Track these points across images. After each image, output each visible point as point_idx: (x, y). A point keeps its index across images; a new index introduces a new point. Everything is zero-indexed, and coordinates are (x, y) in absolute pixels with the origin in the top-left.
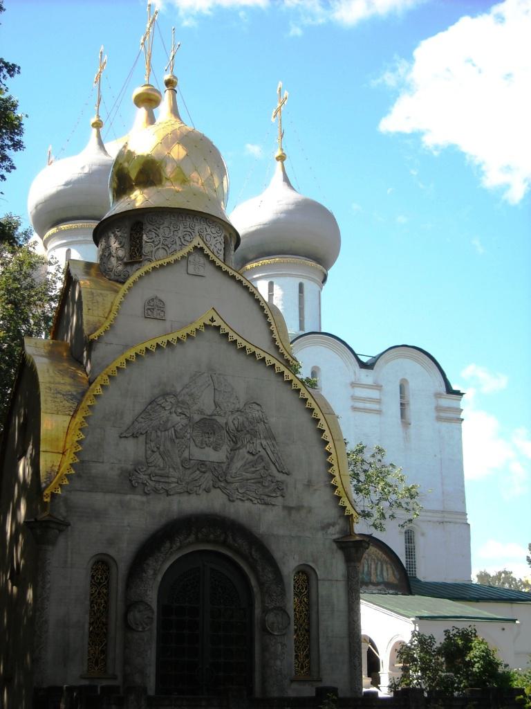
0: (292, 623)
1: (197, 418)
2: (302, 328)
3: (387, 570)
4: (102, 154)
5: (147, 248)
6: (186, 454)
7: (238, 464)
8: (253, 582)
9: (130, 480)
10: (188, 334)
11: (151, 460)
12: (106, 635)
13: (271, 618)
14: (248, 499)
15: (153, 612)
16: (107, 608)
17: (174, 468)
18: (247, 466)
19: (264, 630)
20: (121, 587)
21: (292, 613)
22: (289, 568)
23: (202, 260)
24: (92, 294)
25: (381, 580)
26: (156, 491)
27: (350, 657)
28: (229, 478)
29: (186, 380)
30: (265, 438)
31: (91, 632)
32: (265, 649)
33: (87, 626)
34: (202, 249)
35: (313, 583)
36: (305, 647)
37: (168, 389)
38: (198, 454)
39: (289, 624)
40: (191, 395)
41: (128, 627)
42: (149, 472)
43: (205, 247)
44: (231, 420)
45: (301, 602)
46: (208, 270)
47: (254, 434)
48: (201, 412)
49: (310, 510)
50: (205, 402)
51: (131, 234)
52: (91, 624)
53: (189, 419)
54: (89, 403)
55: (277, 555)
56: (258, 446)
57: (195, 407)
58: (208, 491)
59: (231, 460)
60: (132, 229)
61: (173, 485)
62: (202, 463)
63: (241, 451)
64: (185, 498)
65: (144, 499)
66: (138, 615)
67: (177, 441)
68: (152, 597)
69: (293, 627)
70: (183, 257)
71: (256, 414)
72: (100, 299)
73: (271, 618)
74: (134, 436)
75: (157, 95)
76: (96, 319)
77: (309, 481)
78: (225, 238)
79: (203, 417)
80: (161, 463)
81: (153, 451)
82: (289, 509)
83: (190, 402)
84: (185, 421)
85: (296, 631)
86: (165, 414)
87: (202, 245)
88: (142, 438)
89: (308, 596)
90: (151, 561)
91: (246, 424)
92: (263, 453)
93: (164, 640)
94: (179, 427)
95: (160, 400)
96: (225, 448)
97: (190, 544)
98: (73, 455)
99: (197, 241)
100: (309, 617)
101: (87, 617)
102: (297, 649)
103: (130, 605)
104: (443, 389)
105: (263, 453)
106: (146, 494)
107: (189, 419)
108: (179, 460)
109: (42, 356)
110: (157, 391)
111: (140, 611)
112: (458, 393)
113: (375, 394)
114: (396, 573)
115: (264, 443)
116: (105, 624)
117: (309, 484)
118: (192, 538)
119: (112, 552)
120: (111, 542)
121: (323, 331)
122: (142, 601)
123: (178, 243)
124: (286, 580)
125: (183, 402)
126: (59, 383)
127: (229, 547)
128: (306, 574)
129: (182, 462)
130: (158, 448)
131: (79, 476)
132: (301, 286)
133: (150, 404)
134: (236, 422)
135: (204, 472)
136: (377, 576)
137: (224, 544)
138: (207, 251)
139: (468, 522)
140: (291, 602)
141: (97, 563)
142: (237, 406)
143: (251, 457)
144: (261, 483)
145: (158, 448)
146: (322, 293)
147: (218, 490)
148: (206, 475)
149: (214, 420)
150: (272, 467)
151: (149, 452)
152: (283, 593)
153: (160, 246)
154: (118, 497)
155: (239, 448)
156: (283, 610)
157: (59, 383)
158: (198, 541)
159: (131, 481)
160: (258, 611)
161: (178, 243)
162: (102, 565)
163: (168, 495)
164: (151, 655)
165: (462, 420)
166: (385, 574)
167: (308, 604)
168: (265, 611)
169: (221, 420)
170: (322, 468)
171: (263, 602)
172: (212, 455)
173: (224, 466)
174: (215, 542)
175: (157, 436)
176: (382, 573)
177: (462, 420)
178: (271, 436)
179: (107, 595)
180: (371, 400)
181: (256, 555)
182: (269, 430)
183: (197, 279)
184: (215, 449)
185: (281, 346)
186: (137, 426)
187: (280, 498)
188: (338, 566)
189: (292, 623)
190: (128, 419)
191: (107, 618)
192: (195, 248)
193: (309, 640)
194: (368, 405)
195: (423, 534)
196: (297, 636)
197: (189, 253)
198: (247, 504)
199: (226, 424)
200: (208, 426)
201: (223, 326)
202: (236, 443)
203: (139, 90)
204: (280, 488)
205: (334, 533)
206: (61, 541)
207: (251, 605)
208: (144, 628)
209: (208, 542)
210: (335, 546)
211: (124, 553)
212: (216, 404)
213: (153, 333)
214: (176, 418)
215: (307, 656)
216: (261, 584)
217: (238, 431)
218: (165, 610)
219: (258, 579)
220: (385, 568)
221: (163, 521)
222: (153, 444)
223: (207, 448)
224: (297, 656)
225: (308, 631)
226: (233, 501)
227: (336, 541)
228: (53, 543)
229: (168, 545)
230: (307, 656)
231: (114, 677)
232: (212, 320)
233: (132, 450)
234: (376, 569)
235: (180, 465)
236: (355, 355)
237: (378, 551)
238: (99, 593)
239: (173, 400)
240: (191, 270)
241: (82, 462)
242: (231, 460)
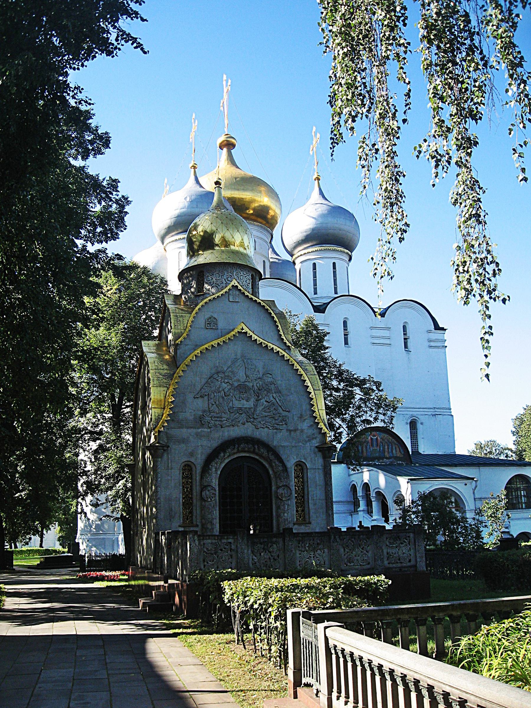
0: (294, 492)
1: (236, 384)
2: (336, 293)
3: (395, 448)
4: (198, 187)
6: (231, 405)
7: (260, 408)
9: (200, 421)
10: (229, 338)
11: (211, 409)
12: (192, 504)
13: (280, 491)
14: (266, 427)
15: (215, 490)
16: (191, 490)
17: (225, 413)
18: (265, 409)
19: (277, 497)
21: (293, 488)
22: (291, 464)
23: (237, 293)
24: (177, 316)
25: (392, 455)
27: (327, 510)
28: (255, 417)
29: (229, 363)
30: (275, 393)
31: (183, 503)
32: (278, 508)
33: (181, 499)
34: (237, 286)
35: (305, 471)
36: (302, 506)
37: (219, 369)
38: (237, 404)
39: (291, 494)
41: (202, 499)
42: (210, 416)
43: (238, 285)
44: (256, 384)
45: (299, 481)
46: (241, 299)
47: (269, 391)
48: (238, 380)
49: (302, 431)
50: (241, 375)
51: (198, 278)
52: (183, 498)
53: (232, 385)
54: (176, 381)
55: (284, 457)
56: (271, 397)
57: (235, 378)
58: (244, 424)
59: (256, 406)
60: (198, 275)
61: (224, 422)
62: (240, 409)
63: (262, 401)
65: (209, 430)
66: (208, 493)
67: (225, 398)
68: (215, 482)
69: (294, 495)
70: (226, 292)
71: (269, 380)
72: (181, 319)
73: (280, 491)
75: (233, 140)
76: (179, 331)
77: (301, 415)
78: (252, 275)
79: (239, 383)
80: (217, 410)
81: (213, 404)
82: (290, 431)
83: (232, 376)
84: (229, 387)
85: (296, 497)
87: (237, 284)
88: (206, 398)
89: (303, 478)
90: (213, 464)
91: (264, 385)
92: (274, 401)
93: (223, 504)
94: (226, 390)
95: (215, 376)
96: (253, 400)
97: (234, 453)
98: (169, 410)
99: (234, 282)
100: (303, 489)
101: (181, 495)
102: (297, 507)
103: (203, 488)
104: (433, 327)
105: (274, 401)
106: (210, 428)
108: (227, 409)
109: (153, 353)
110: (213, 371)
111: (208, 491)
112: (443, 329)
113: (386, 333)
114: (402, 450)
115: (274, 395)
116: (192, 498)
117: (301, 417)
118: (235, 451)
119: (193, 460)
120: (192, 454)
121: (350, 294)
122: (209, 486)
123: (224, 282)
124: (289, 470)
125: (228, 376)
126: (160, 369)
127: (257, 454)
128: (301, 466)
129: (229, 409)
130: (215, 402)
131: (172, 420)
132: (334, 264)
133: (210, 378)
134: (258, 385)
135: (241, 414)
136: (389, 453)
137: (254, 452)
138: (240, 287)
139: (452, 414)
140: (293, 482)
141: (185, 466)
142: (259, 376)
143: (267, 403)
144: (273, 418)
145: (215, 402)
146: (349, 268)
147: (250, 423)
148: (243, 415)
149: (246, 384)
150: (280, 408)
151: (210, 405)
152: (288, 477)
153: (214, 285)
154: (194, 431)
155: (261, 399)
156: (288, 487)
157: (160, 369)
158: (239, 452)
159: (201, 421)
160: (273, 488)
161: (224, 282)
162: (188, 468)
163: (222, 427)
164: (216, 513)
165: (446, 347)
166: (394, 451)
167: (303, 482)
170: (308, 407)
171: (277, 482)
173: (252, 410)
174: (248, 452)
175: (215, 396)
176: (392, 451)
177: (446, 347)
178: (278, 391)
179: (191, 482)
180: (383, 337)
181: (272, 457)
182: (277, 388)
183: (235, 304)
184: (247, 401)
185: (284, 338)
186: (203, 391)
187: (284, 426)
188: (319, 461)
189: (294, 492)
191: (192, 495)
192: (233, 286)
193: (303, 502)
194: (382, 341)
195: (422, 424)
196: (297, 500)
197: (229, 289)
198: (266, 429)
199: (253, 386)
200: (242, 389)
201: (249, 331)
202: (259, 397)
203: (222, 138)
204: (284, 420)
205: (316, 443)
208: (211, 499)
209: (245, 452)
210: (316, 450)
211: (199, 460)
215: (303, 511)
216: (275, 473)
217: (260, 390)
218: (222, 489)
219: (273, 471)
220: (394, 448)
222: (212, 400)
223: (242, 401)
224: (297, 511)
225: (303, 497)
226: (258, 429)
227: (316, 447)
228: (162, 457)
229: (222, 454)
230: (303, 511)
231: (197, 526)
232: (242, 329)
233: (201, 404)
234: (388, 448)
235: (227, 411)
236: (372, 308)
237: (389, 437)
238: (187, 482)
239: (223, 376)
241: (173, 413)
242: (256, 406)
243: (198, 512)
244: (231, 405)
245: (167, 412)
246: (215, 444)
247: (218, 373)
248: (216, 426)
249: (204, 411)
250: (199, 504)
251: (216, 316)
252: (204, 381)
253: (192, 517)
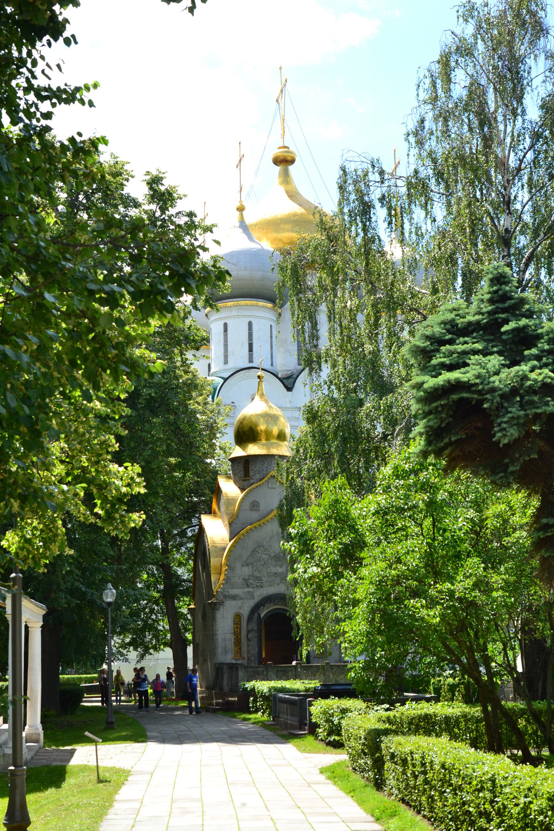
1: (273, 555)
5: (251, 473)
6: (269, 570)
9: (247, 583)
12: (240, 643)
16: (240, 632)
26: (257, 586)
29: (268, 539)
38: (274, 570)
40: (270, 546)
48: (274, 552)
53: (270, 556)
58: (278, 584)
62: (276, 573)
64: (269, 588)
74: (247, 565)
86: (259, 555)
88: (250, 566)
95: (257, 549)
107: (270, 556)
119: (241, 612)
162: (238, 617)
184: (281, 567)
190: (245, 558)
206: (221, 608)
211: (245, 612)
213: (254, 515)
214: (264, 556)
221: (261, 598)
233: (247, 571)
240: (270, 486)
243: (245, 649)
244: (269, 570)
245: (222, 577)
246: (257, 599)
247: (259, 547)
248: (257, 586)
249: (250, 576)
250: (246, 643)
251: (257, 500)
252: (249, 554)
253: (241, 652)
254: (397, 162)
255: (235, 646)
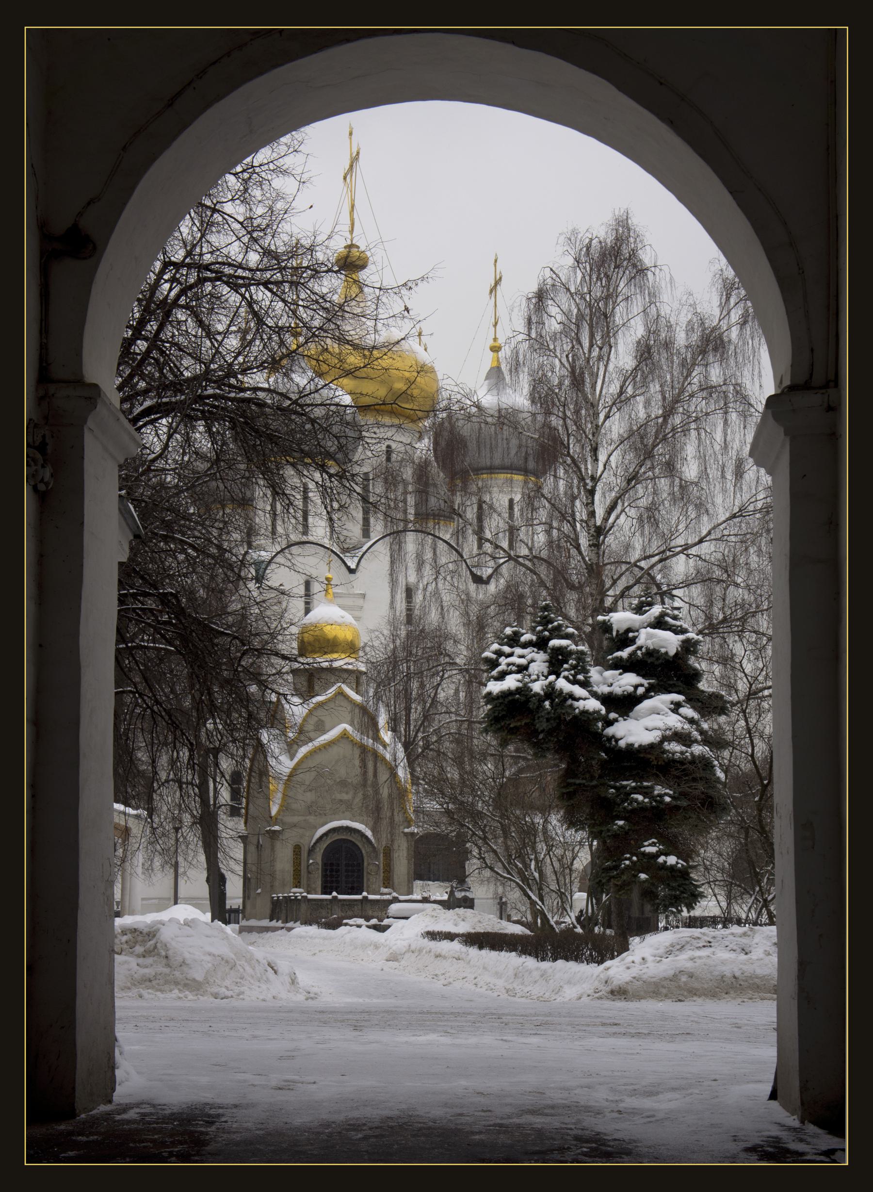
1: (338, 780)
8: (364, 852)
13: (371, 867)
20: (306, 855)
23: (342, 698)
26: (320, 814)
32: (368, 880)
41: (309, 872)
58: (343, 812)
59: (354, 798)
62: (341, 801)
74: (310, 791)
119: (302, 841)
154: (304, 818)
160: (365, 864)
168: (368, 864)
169: (350, 781)
172: (345, 797)
184: (347, 793)
190: (307, 783)
207: (363, 861)
212: (347, 774)
214: (329, 781)
233: (310, 797)
242: (354, 798)
248: (320, 814)
249: (313, 802)
252: (312, 778)
254: (498, 277)
255: (294, 879)
